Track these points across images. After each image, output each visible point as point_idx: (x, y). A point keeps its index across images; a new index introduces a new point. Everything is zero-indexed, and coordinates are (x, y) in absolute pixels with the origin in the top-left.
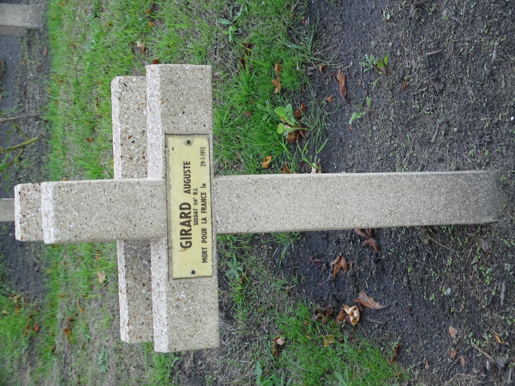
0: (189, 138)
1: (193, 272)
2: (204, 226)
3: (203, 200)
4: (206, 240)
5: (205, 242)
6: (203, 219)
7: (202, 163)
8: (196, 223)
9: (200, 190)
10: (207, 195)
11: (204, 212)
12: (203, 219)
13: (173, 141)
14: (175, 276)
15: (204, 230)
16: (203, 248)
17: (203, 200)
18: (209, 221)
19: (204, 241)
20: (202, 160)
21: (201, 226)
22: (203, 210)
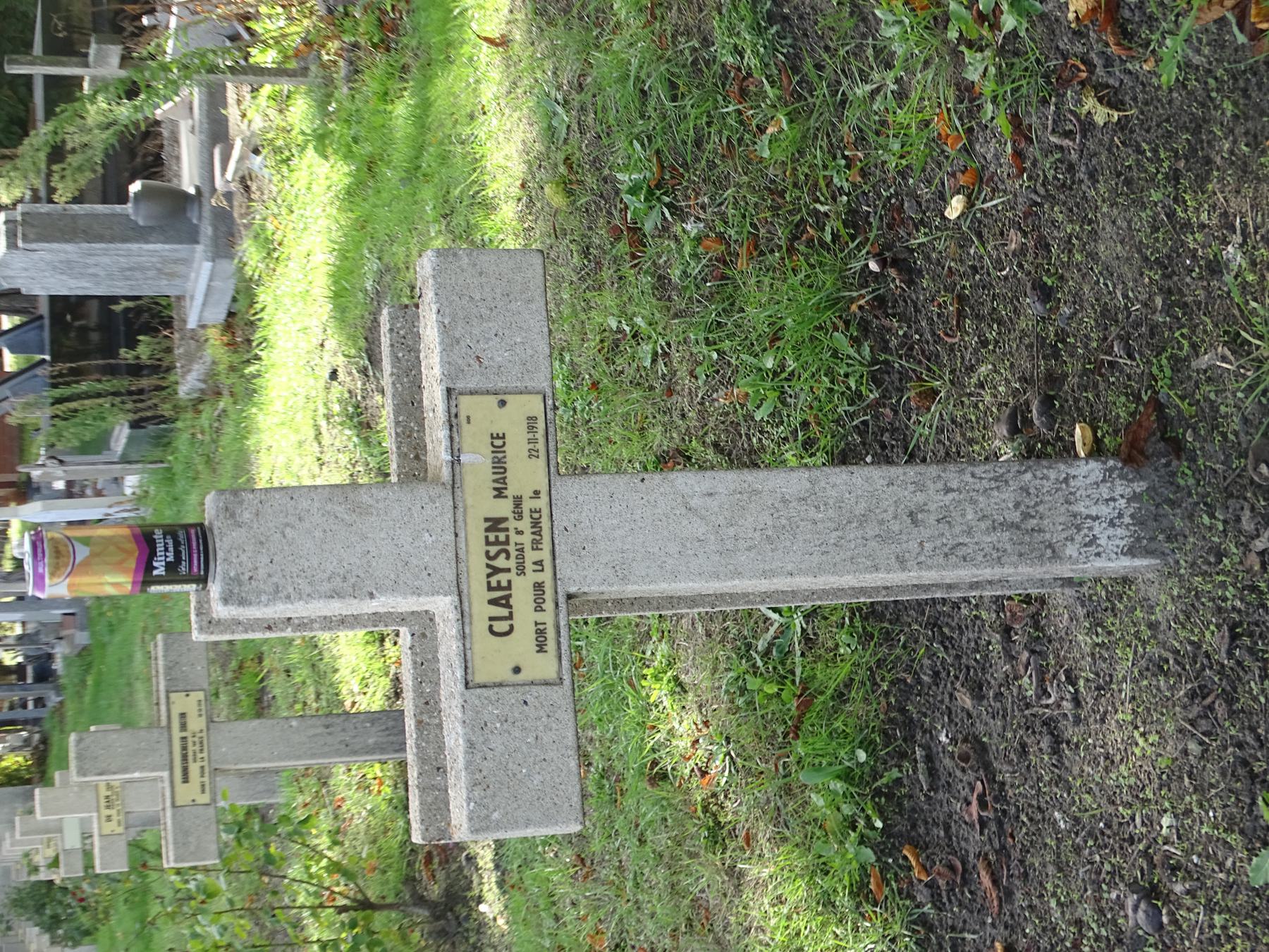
0: (500, 397)
2: (539, 577)
3: (536, 524)
5: (543, 610)
6: (535, 563)
8: (521, 571)
9: (527, 505)
11: (537, 549)
12: (535, 563)
14: (480, 678)
16: (536, 624)
17: (536, 524)
19: (539, 608)
20: (531, 446)
21: (532, 577)
22: (536, 545)
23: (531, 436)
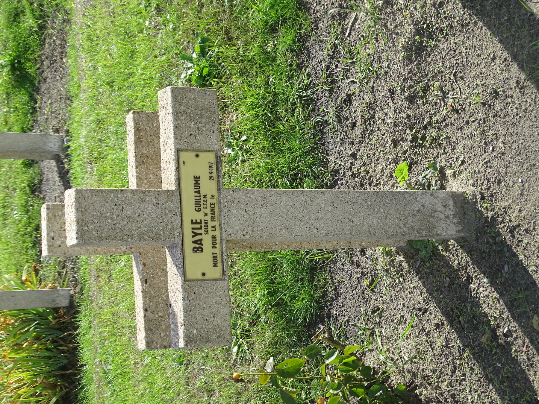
1: (204, 274)
2: (214, 233)
3: (213, 210)
4: (216, 246)
6: (212, 227)
7: (211, 178)
9: (209, 201)
10: (215, 205)
11: (213, 221)
12: (212, 227)
13: (184, 156)
15: (214, 237)
16: (213, 254)
18: (218, 227)
19: (214, 247)
20: (211, 175)
21: (211, 233)
22: (213, 219)
23: (210, 171)
